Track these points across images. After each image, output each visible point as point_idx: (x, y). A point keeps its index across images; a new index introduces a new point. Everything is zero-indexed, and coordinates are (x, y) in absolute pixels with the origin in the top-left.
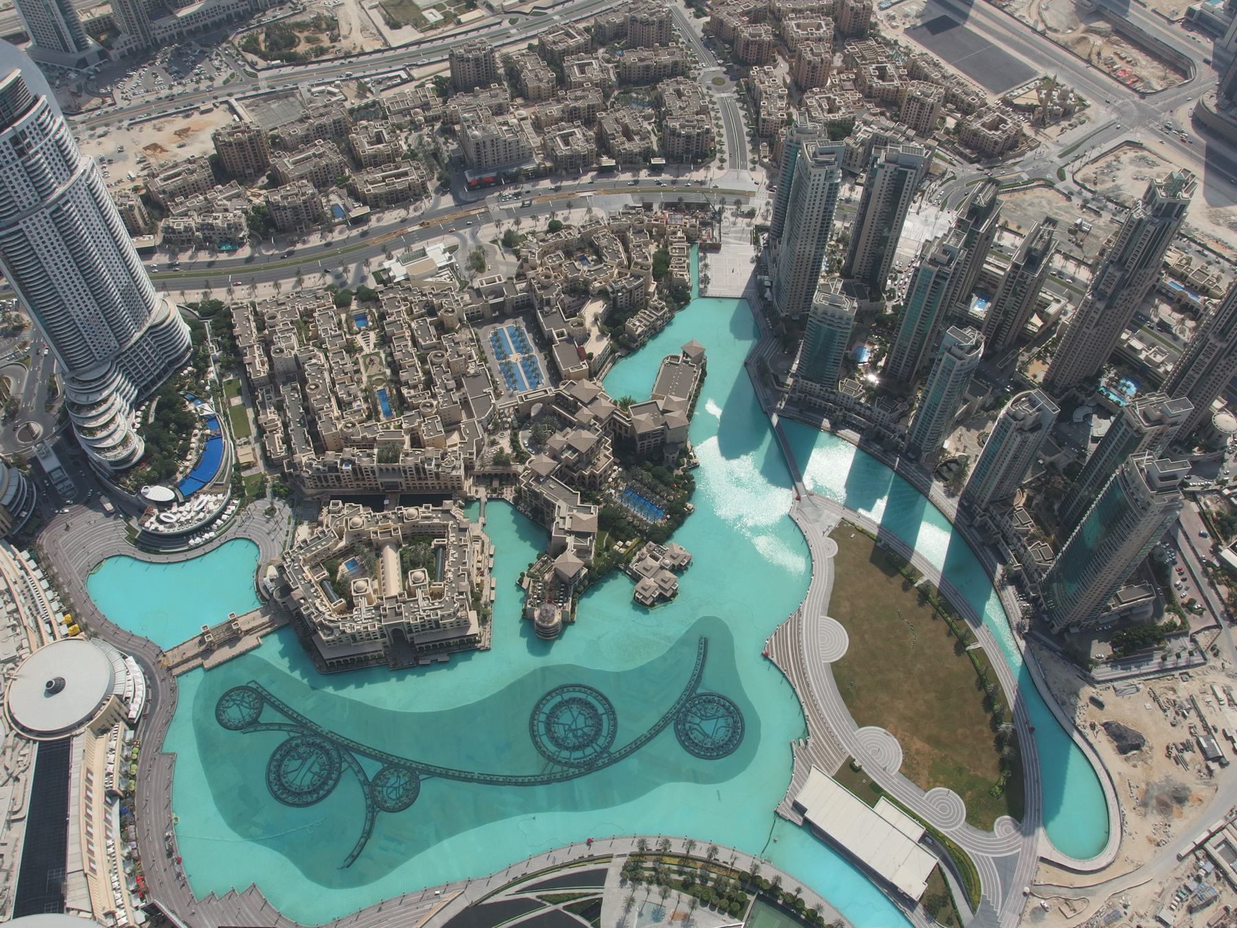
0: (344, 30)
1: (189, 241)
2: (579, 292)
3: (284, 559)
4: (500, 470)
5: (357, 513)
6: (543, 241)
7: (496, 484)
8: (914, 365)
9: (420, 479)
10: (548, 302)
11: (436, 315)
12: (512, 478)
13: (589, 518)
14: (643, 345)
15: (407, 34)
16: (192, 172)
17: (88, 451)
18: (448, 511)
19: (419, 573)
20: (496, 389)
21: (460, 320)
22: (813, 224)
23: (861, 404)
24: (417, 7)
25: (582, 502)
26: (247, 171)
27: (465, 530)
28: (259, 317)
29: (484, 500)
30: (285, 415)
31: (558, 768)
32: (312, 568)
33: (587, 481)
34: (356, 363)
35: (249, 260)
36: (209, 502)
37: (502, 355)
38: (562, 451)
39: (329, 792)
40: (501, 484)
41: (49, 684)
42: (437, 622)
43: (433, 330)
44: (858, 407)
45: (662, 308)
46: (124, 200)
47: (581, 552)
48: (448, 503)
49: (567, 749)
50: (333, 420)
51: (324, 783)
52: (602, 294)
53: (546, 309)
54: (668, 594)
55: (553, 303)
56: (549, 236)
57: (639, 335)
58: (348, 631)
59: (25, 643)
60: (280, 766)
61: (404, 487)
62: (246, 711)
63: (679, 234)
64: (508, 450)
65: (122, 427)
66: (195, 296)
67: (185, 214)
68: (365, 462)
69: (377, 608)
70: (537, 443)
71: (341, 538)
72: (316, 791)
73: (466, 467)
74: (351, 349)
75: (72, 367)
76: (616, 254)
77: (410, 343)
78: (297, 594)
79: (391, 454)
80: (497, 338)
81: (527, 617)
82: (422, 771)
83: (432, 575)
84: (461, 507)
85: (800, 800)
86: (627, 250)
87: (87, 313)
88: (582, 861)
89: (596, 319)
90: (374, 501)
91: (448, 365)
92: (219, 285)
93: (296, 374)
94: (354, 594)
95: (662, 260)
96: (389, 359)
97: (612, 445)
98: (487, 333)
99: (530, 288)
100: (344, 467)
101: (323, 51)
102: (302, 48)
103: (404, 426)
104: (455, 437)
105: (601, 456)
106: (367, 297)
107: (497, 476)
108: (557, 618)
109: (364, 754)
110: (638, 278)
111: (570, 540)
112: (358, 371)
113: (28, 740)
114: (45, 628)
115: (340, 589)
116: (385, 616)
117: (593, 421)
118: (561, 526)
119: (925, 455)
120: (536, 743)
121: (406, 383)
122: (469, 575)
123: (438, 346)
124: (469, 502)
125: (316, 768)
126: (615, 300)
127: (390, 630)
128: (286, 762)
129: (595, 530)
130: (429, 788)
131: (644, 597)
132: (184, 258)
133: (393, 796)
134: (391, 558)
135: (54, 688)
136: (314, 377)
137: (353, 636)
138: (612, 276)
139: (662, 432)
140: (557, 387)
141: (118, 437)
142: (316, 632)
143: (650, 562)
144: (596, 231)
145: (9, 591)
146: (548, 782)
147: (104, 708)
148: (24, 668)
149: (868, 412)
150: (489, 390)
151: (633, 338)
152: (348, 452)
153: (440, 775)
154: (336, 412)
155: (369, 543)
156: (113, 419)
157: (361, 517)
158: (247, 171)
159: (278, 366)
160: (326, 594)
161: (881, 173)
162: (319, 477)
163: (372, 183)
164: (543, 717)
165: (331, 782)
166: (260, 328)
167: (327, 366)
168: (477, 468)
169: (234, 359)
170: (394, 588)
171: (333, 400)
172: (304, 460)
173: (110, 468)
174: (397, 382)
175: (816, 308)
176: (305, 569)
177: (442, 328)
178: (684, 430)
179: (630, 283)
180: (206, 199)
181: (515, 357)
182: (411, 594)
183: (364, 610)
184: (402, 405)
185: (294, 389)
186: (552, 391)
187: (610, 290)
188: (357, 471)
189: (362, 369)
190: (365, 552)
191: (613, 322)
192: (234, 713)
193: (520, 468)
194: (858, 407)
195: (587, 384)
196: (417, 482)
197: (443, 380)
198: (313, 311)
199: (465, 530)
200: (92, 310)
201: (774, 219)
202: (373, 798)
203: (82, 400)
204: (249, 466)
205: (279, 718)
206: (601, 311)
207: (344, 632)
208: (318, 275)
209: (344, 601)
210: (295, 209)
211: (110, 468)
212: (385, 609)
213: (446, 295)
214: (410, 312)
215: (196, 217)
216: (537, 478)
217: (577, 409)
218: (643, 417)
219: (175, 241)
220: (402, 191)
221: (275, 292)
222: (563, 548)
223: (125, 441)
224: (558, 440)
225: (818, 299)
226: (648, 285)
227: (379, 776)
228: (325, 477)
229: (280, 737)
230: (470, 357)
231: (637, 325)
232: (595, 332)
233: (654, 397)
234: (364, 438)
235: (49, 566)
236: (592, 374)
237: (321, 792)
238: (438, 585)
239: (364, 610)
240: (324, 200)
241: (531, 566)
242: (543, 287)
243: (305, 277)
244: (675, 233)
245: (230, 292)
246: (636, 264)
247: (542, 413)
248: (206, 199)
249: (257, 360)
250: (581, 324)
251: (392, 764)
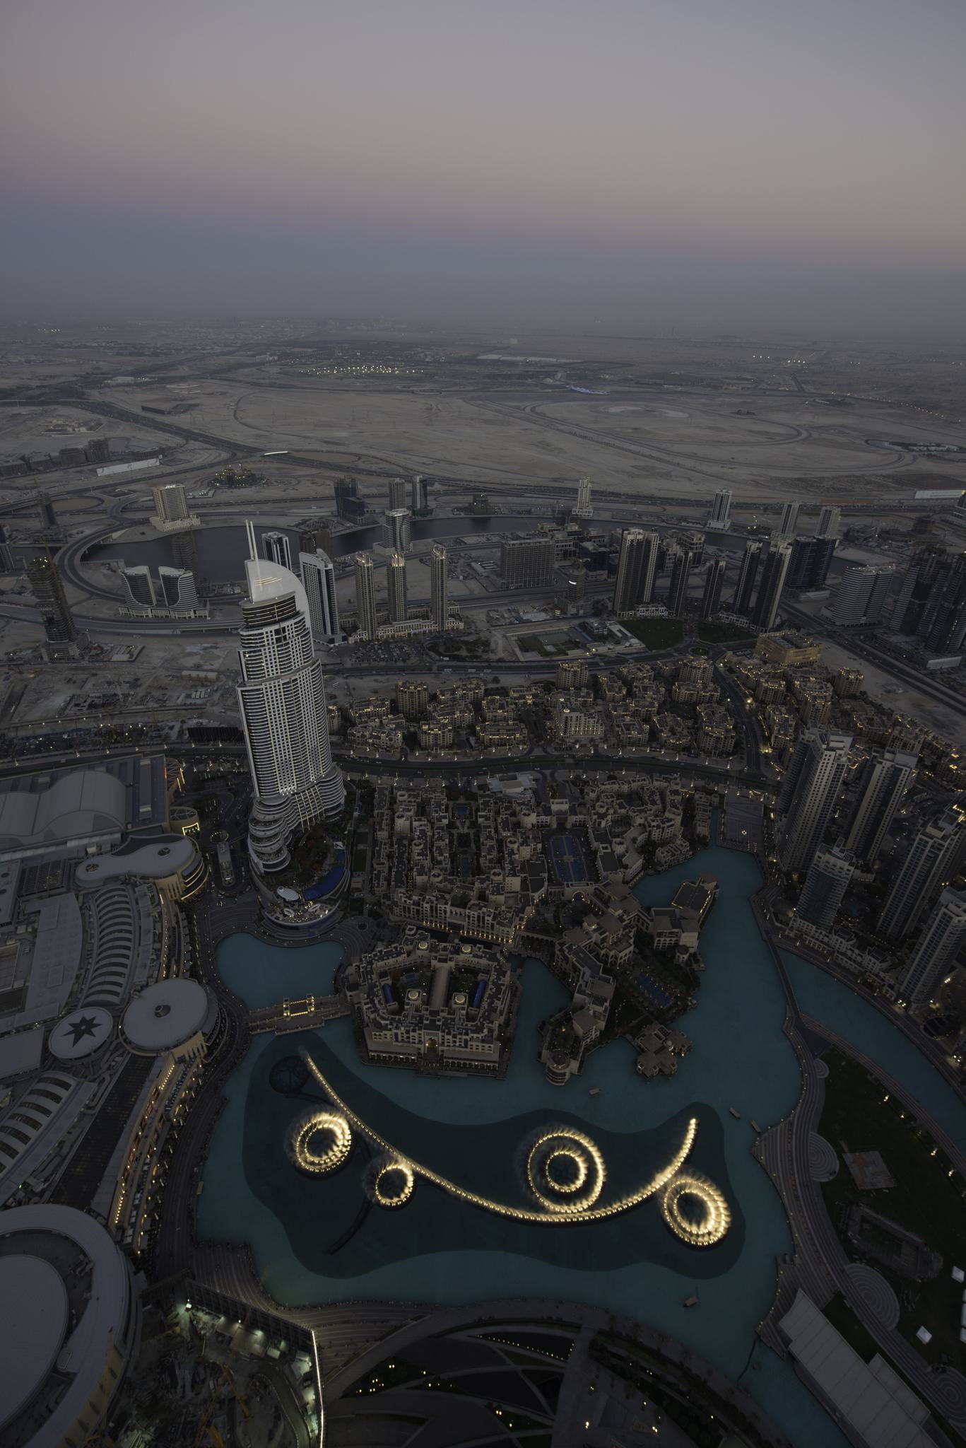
0: (493, 646)
5: (424, 939)
8: (903, 927)
13: (608, 990)
15: (533, 656)
20: (550, 876)
24: (542, 645)
36: (320, 911)
54: (667, 1071)
59: (155, 974)
64: (551, 921)
66: (357, 777)
83: (471, 1003)
88: (548, 1322)
90: (440, 936)
101: (476, 657)
102: (464, 653)
106: (472, 797)
119: (914, 1006)
126: (650, 833)
145: (161, 935)
148: (146, 993)
149: (859, 959)
150: (546, 875)
161: (879, 767)
173: (263, 870)
184: (478, 871)
204: (358, 890)
223: (279, 852)
238: (473, 1011)
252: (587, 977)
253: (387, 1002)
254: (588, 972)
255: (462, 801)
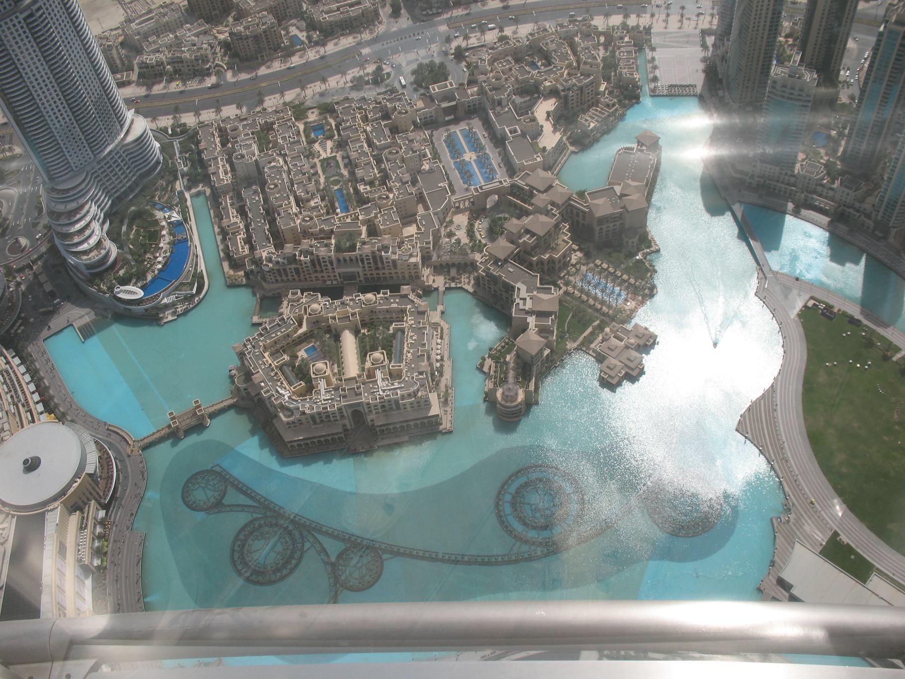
1: (161, 75)
2: (532, 92)
3: (245, 345)
4: (457, 259)
6: (492, 48)
7: (453, 272)
9: (377, 268)
10: (500, 103)
11: (389, 118)
12: (473, 266)
13: (550, 299)
14: (596, 140)
16: (164, 15)
17: (64, 253)
18: (406, 296)
19: (377, 355)
20: (450, 185)
21: (414, 123)
22: (761, 29)
23: (823, 186)
25: (541, 284)
26: (213, 13)
27: (423, 313)
28: (222, 132)
29: (442, 289)
30: (247, 216)
31: (525, 548)
32: (271, 355)
33: (546, 268)
34: (314, 166)
35: (214, 87)
37: (456, 152)
38: (520, 237)
39: (292, 571)
40: (458, 271)
41: (26, 462)
42: (397, 402)
43: (387, 131)
44: (819, 189)
45: (614, 105)
46: (104, 42)
47: (543, 331)
48: (405, 289)
49: (534, 528)
50: (292, 217)
51: (288, 562)
52: (553, 93)
53: (498, 109)
54: (634, 373)
55: (504, 103)
56: (498, 45)
57: (592, 130)
58: (307, 412)
60: (243, 545)
61: (362, 278)
62: (210, 493)
63: (626, 39)
64: (465, 240)
65: (97, 232)
66: (166, 121)
67: (157, 51)
68: (322, 252)
69: (336, 389)
70: (493, 233)
71: (300, 325)
72: (278, 570)
73: (423, 258)
74: (310, 155)
75: (51, 179)
76: (564, 57)
77: (365, 145)
78: (259, 376)
79: (348, 241)
80: (451, 143)
81: (489, 398)
82: (385, 551)
84: (419, 296)
85: (787, 576)
86: (575, 53)
87: (62, 122)
89: (547, 119)
90: (334, 293)
91: (403, 160)
92: (187, 111)
93: (256, 178)
94: (313, 376)
95: (610, 65)
96: (346, 161)
97: (569, 230)
98: (441, 135)
99: (482, 92)
100: (302, 258)
103: (361, 217)
104: (411, 230)
105: (560, 242)
107: (455, 267)
108: (521, 396)
109: (326, 534)
110: (589, 76)
111: (532, 320)
112: (316, 173)
113: (8, 515)
114: (26, 416)
115: (302, 373)
116: (345, 397)
117: (550, 207)
118: (521, 307)
119: (894, 231)
120: (502, 523)
121: (363, 180)
122: (429, 358)
123: (394, 144)
124: (428, 292)
125: (279, 548)
126: (566, 97)
127: (350, 411)
128: (250, 541)
129: (555, 308)
130: (393, 566)
131: (610, 376)
132: (158, 89)
133: (356, 575)
134: (349, 342)
135: (31, 465)
136: (274, 178)
137: (313, 417)
138: (562, 75)
139: (620, 216)
140: (511, 176)
141: (93, 241)
142: (276, 416)
143: (614, 342)
144: (544, 38)
146: (516, 561)
147: (75, 485)
151: (586, 134)
152: (306, 243)
153: (404, 555)
154: (295, 209)
155: (328, 330)
156: (87, 226)
157: (319, 305)
158: (213, 13)
159: (240, 172)
160: (286, 378)
162: (280, 271)
163: (327, 13)
164: (508, 497)
165: (294, 562)
166: (224, 144)
167: (286, 168)
168: (434, 258)
169: (200, 173)
170: (352, 368)
171: (292, 198)
172: (264, 255)
173: (86, 272)
174: (354, 179)
175: (775, 82)
176: (266, 355)
177: (395, 130)
178: (643, 214)
179: (580, 81)
180: (176, 37)
181: (469, 156)
182: (371, 375)
183: (323, 391)
185: (256, 192)
186: (507, 182)
187: (560, 87)
188: (316, 262)
189: (320, 171)
190: (325, 336)
191: (564, 117)
192: (200, 495)
193: (478, 257)
194: (819, 189)
195: (542, 173)
196: (374, 272)
197: (399, 174)
198: (273, 123)
199: (423, 313)
200: (67, 119)
201: (722, 19)
202: (336, 579)
203: (61, 208)
205: (242, 500)
206: (553, 108)
207: (304, 413)
208: (278, 96)
209: (303, 384)
210: (256, 38)
211: (86, 272)
212: (344, 390)
213: (399, 100)
214: (365, 119)
215: (166, 53)
216: (496, 261)
217: (532, 195)
218: (600, 201)
219: (150, 75)
220: (356, 18)
221: (238, 112)
222: (524, 328)
223: (99, 244)
224: (514, 224)
225: (776, 71)
226: (599, 85)
227: (340, 556)
228: (285, 270)
229: (242, 518)
230: (425, 155)
231: (590, 122)
232: (548, 127)
233: (610, 184)
234: (322, 230)
235: (33, 362)
236: (548, 167)
237: (285, 572)
239: (323, 391)
240: (283, 33)
241: (491, 349)
242: (494, 89)
243: (267, 98)
244: (622, 38)
245: (197, 114)
246: (585, 63)
247: (497, 205)
248: (176, 37)
249: (221, 170)
250: (534, 120)
251: (354, 544)
252: (523, 294)
253: (290, 384)
254: (523, 288)
255: (312, 117)
